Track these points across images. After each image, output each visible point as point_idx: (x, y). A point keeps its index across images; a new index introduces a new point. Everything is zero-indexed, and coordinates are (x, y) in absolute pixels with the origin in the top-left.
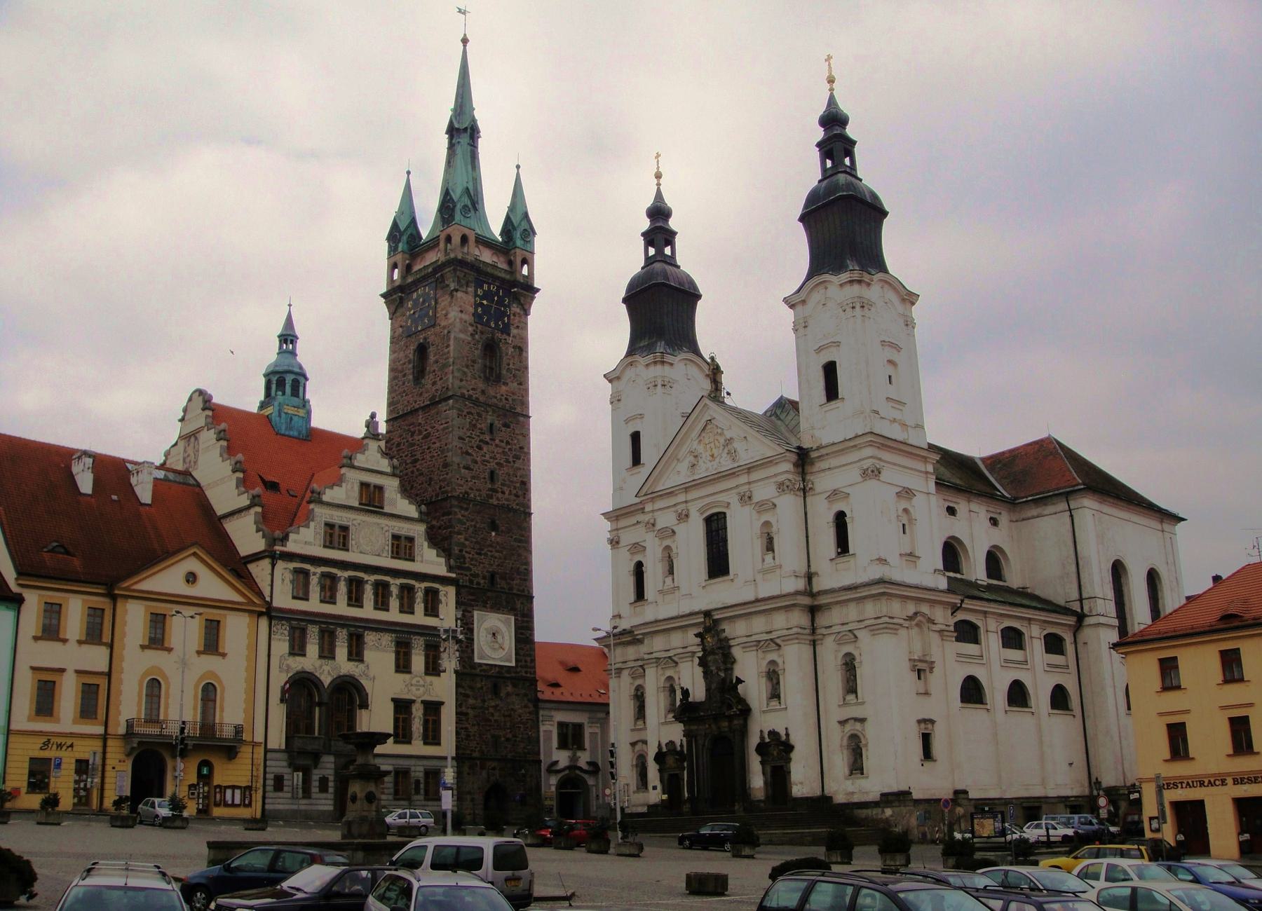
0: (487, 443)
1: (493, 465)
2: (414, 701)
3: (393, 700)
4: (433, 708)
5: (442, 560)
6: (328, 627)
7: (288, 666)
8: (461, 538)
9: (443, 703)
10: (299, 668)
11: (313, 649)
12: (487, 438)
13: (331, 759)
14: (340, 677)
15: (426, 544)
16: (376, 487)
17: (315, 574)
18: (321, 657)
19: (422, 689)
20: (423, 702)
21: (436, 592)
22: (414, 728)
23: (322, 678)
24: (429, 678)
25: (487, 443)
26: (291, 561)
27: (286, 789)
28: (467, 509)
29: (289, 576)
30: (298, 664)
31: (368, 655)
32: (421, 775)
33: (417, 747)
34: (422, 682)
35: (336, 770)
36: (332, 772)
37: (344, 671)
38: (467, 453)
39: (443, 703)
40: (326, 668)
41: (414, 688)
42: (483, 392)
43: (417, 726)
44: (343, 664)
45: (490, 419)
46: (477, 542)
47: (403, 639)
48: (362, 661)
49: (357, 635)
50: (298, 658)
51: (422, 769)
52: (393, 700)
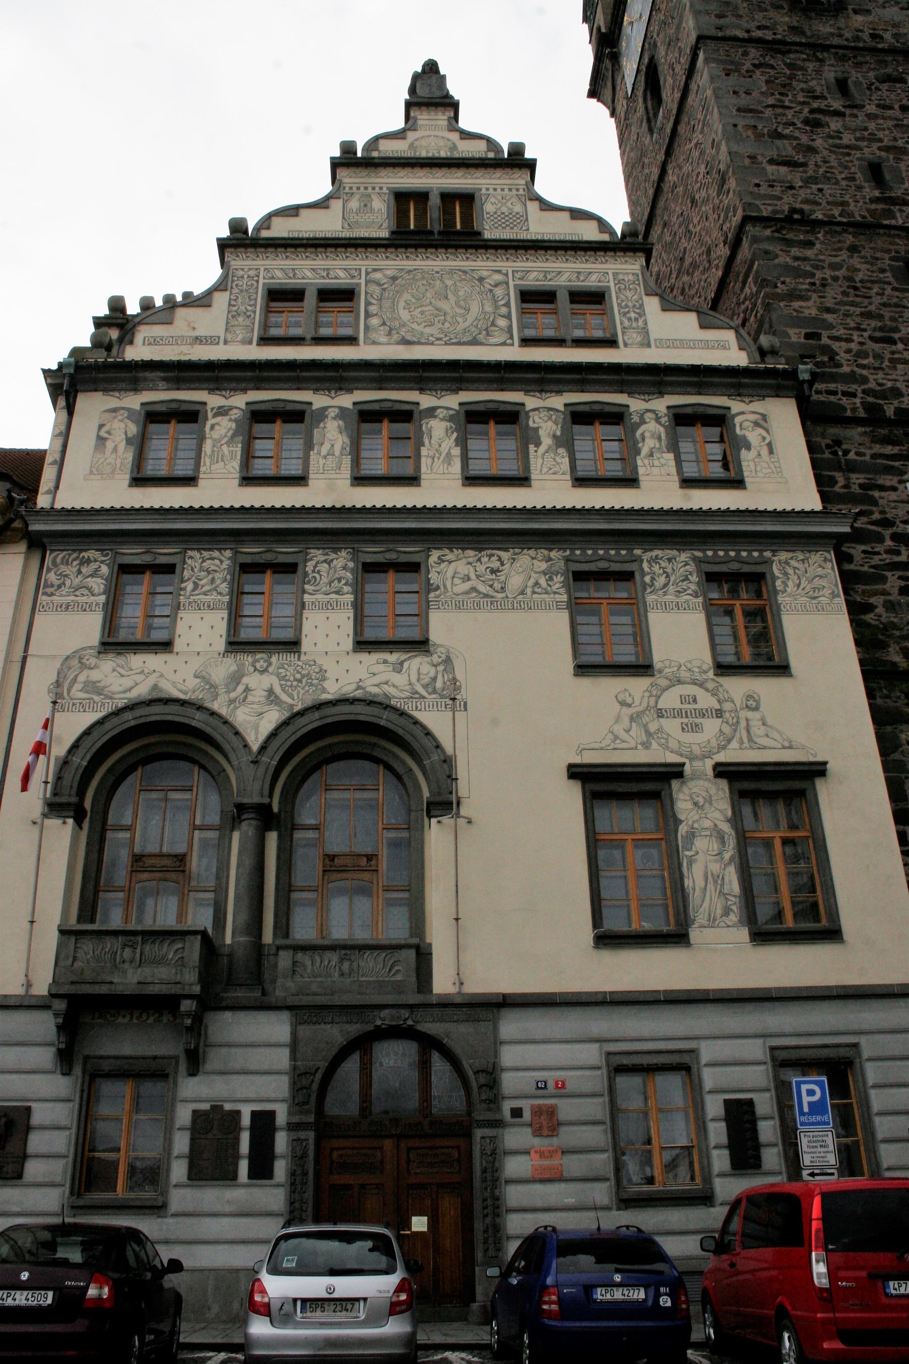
0: (837, 114)
1: (871, 152)
2: (675, 772)
3: (576, 772)
4: (778, 790)
5: (729, 336)
6: (268, 550)
7: (93, 687)
8: (810, 308)
9: (818, 770)
10: (142, 691)
11: (201, 630)
12: (837, 104)
13: (276, 1028)
14: (319, 706)
15: (652, 304)
16: (448, 198)
17: (222, 412)
18: (235, 645)
19: (711, 726)
20: (723, 771)
21: (718, 420)
22: (695, 878)
23: (241, 717)
24: (738, 687)
25: (837, 114)
26: (135, 386)
27: (33, 1169)
28: (810, 244)
29: (123, 429)
30: (132, 679)
31: (441, 627)
32: (755, 1081)
33: (722, 956)
34: (706, 701)
35: (299, 1078)
36: (280, 1086)
37: (332, 690)
38: (778, 136)
39: (818, 770)
40: (258, 683)
41: (672, 726)
42: (793, 29)
43: (709, 866)
44: (333, 660)
45: (830, 74)
46: (868, 315)
47: (599, 561)
48: (420, 645)
49: (392, 553)
50: (138, 660)
51: (756, 1049)
52: (576, 772)
